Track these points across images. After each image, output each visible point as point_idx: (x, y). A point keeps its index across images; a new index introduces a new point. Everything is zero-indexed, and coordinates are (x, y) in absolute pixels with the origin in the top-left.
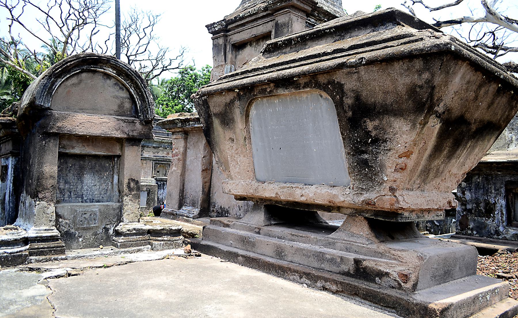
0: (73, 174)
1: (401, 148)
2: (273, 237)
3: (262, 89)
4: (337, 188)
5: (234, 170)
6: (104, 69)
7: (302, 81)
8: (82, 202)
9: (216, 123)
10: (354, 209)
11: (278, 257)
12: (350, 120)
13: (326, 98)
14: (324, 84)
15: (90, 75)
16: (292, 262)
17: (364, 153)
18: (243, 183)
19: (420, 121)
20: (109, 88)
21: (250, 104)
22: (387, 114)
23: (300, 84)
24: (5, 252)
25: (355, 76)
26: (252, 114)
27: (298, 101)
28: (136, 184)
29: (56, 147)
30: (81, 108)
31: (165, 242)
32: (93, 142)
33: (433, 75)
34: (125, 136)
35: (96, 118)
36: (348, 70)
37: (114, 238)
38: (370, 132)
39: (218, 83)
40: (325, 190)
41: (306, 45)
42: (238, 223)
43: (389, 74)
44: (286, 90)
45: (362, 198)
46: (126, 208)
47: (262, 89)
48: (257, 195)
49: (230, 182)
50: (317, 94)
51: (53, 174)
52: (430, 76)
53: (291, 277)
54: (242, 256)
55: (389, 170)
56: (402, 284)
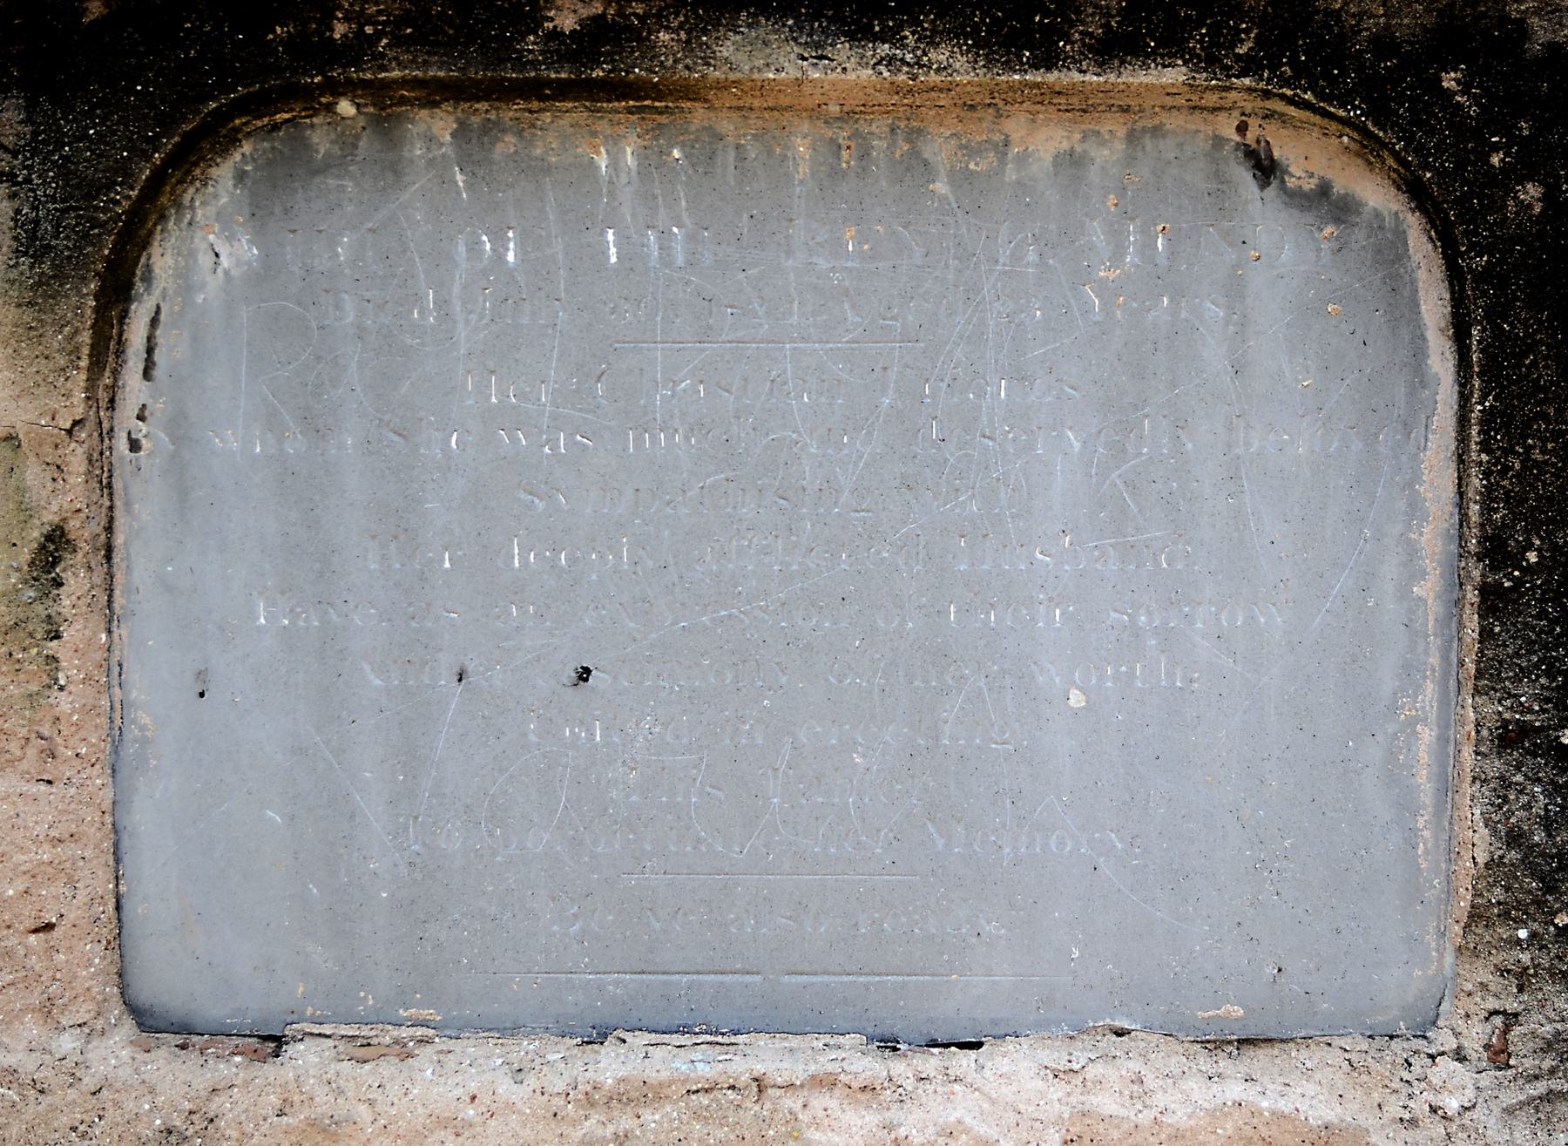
13: (1324, 190)
14: (1383, 44)
27: (941, 187)
50: (1218, 141)
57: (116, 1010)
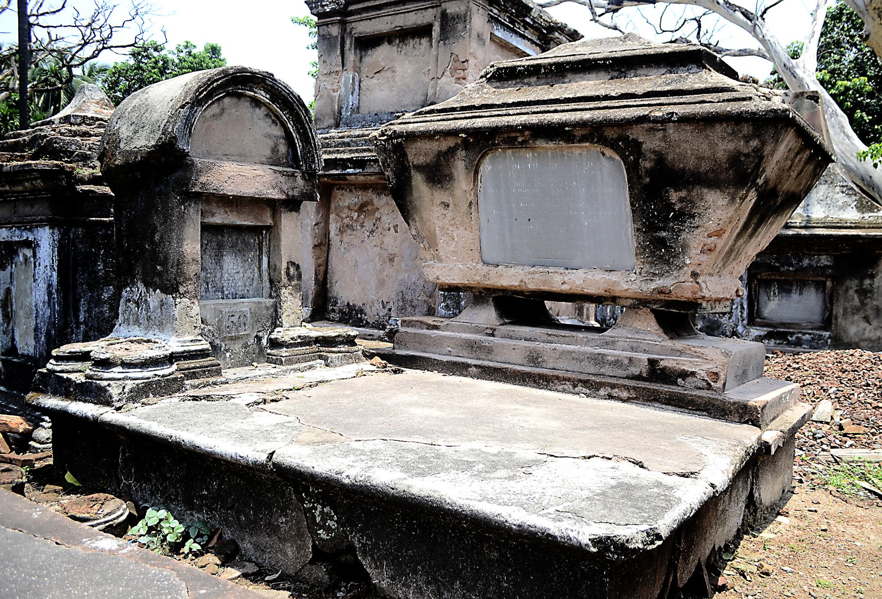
0: (210, 256)
1: (712, 226)
2: (517, 339)
3: (508, 137)
4: (616, 272)
5: (444, 246)
6: (255, 93)
7: (579, 132)
8: (223, 298)
9: (418, 180)
10: (636, 299)
11: (533, 365)
12: (645, 187)
14: (612, 139)
15: (235, 100)
16: (555, 369)
17: (660, 230)
18: (461, 266)
19: (741, 195)
20: (259, 121)
21: (483, 157)
22: (698, 184)
23: (575, 136)
24: (156, 375)
25: (660, 135)
26: (484, 170)
28: (297, 270)
29: (197, 214)
30: (225, 153)
31: (343, 354)
32: (237, 206)
33: (763, 143)
34: (284, 197)
35: (248, 169)
36: (651, 125)
37: (269, 351)
38: (674, 204)
39: (416, 120)
40: (600, 276)
41: (564, 76)
42: (454, 322)
43: (707, 137)
44: (550, 142)
45: (653, 286)
46: (284, 306)
47: (508, 137)
48: (487, 283)
49: (438, 265)
51: (195, 256)
52: (759, 143)
53: (560, 388)
54: (476, 366)
55: (694, 251)
56: (712, 384)
57: (480, 261)
